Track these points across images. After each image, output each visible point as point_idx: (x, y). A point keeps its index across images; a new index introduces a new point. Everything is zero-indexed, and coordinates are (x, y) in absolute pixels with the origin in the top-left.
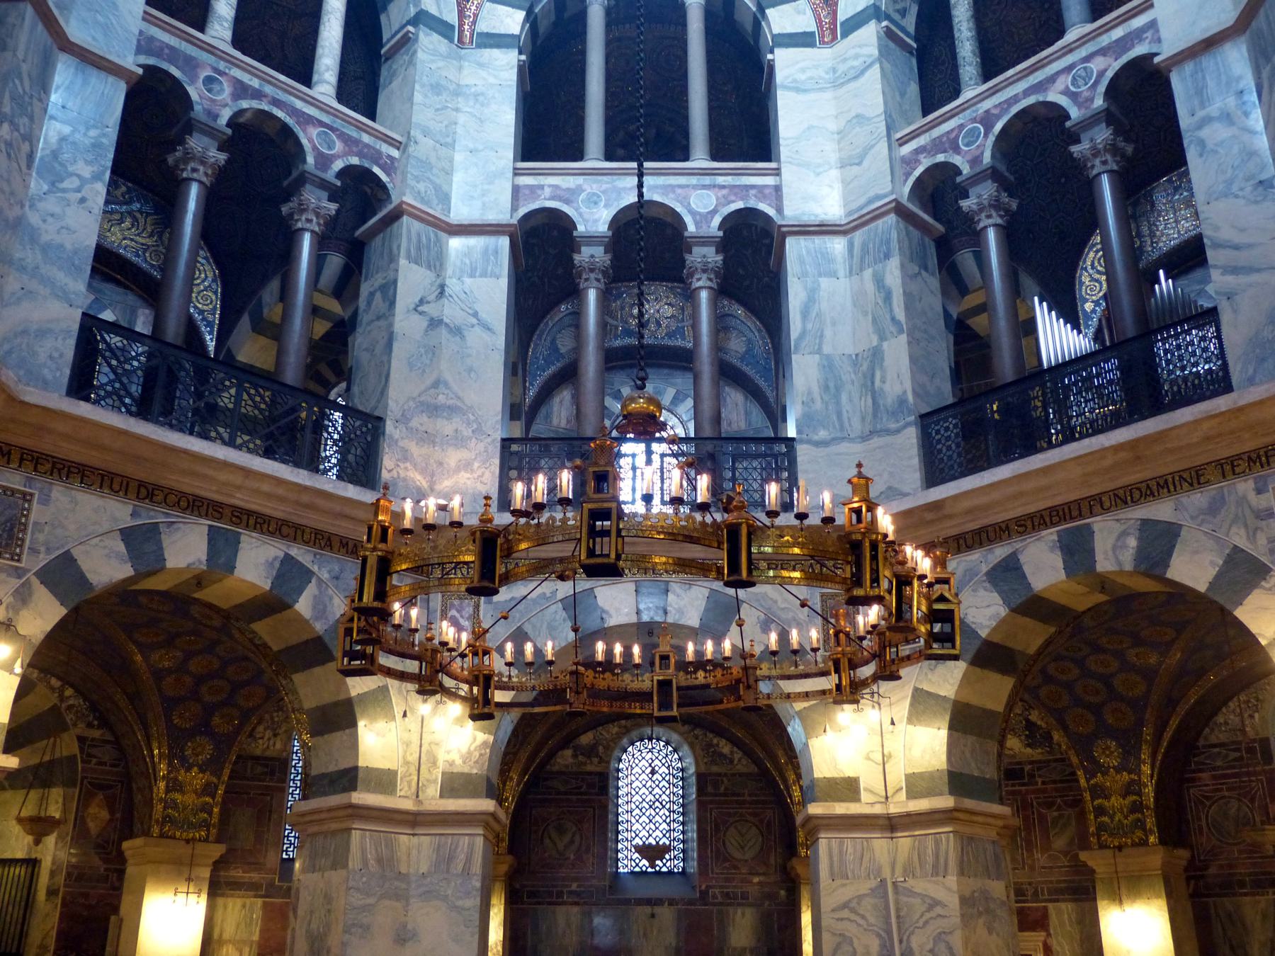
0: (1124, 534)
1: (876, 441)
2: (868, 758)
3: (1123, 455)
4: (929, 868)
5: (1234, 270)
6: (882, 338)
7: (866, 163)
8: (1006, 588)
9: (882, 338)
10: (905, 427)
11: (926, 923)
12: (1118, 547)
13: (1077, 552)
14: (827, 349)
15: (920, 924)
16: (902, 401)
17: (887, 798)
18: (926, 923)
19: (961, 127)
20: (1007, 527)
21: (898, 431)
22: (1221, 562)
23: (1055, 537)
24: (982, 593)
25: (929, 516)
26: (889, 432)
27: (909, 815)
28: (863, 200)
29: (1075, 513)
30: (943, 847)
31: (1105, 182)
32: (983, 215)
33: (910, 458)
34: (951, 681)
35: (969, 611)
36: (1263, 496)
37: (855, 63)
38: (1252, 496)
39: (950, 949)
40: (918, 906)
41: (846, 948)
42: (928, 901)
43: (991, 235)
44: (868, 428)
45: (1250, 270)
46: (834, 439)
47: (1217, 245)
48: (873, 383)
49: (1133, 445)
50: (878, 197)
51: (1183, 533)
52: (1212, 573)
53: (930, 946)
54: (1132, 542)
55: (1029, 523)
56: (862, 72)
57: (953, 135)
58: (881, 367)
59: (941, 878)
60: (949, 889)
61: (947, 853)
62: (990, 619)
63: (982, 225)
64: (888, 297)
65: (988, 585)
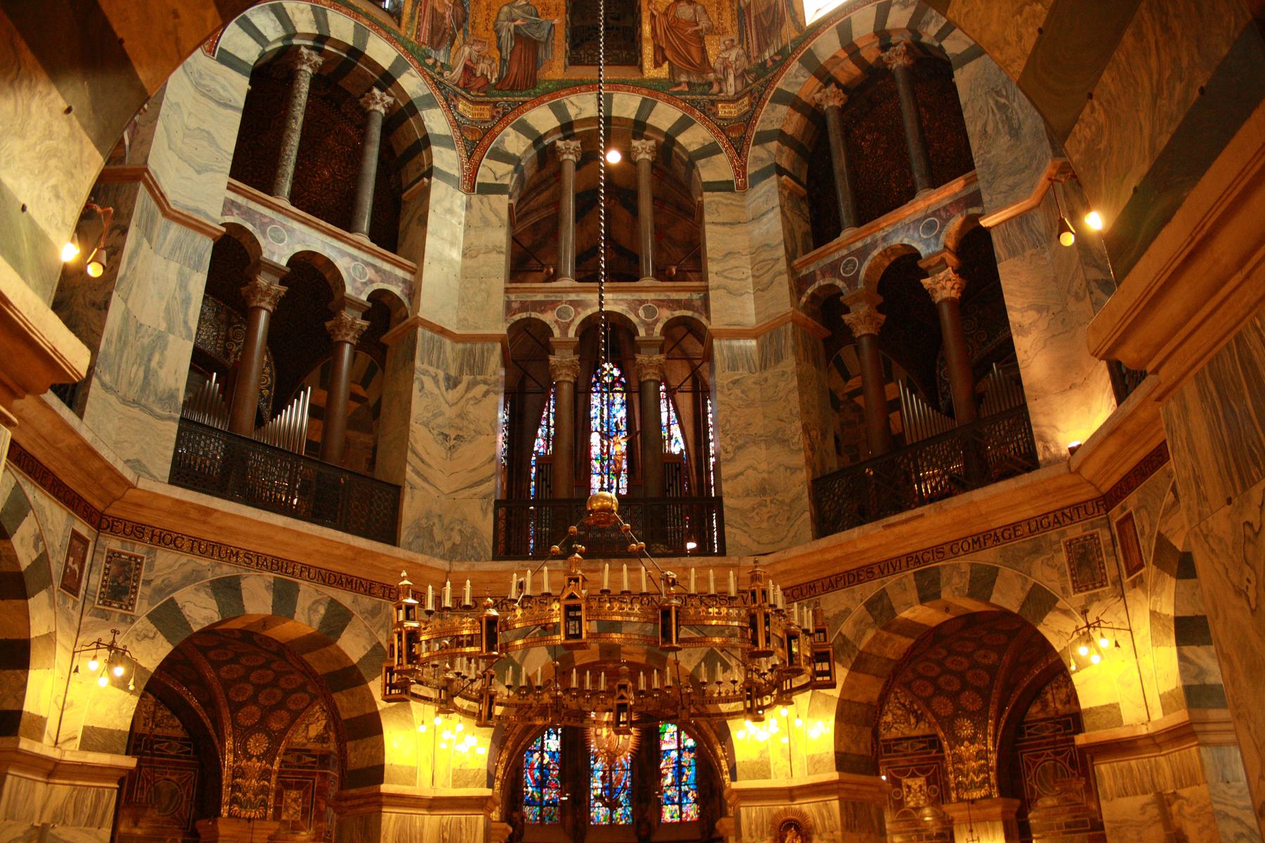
1: (136, 412)
3: (350, 553)
5: (418, 473)
6: (170, 329)
7: (206, 177)
9: (170, 329)
10: (171, 418)
12: (312, 609)
13: (285, 597)
14: (130, 305)
16: (172, 396)
19: (272, 221)
21: (162, 418)
24: (203, 595)
25: (193, 514)
26: (152, 413)
27: (83, 765)
28: (191, 204)
29: (290, 570)
31: (347, 347)
32: (268, 299)
33: (166, 448)
37: (221, 91)
43: (263, 316)
44: (132, 394)
45: (425, 480)
46: (111, 388)
47: (414, 452)
48: (150, 360)
49: (360, 552)
50: (207, 216)
52: (362, 653)
54: (322, 611)
55: (254, 559)
56: (226, 105)
57: (267, 220)
58: (162, 354)
62: (204, 618)
63: (263, 304)
64: (187, 301)
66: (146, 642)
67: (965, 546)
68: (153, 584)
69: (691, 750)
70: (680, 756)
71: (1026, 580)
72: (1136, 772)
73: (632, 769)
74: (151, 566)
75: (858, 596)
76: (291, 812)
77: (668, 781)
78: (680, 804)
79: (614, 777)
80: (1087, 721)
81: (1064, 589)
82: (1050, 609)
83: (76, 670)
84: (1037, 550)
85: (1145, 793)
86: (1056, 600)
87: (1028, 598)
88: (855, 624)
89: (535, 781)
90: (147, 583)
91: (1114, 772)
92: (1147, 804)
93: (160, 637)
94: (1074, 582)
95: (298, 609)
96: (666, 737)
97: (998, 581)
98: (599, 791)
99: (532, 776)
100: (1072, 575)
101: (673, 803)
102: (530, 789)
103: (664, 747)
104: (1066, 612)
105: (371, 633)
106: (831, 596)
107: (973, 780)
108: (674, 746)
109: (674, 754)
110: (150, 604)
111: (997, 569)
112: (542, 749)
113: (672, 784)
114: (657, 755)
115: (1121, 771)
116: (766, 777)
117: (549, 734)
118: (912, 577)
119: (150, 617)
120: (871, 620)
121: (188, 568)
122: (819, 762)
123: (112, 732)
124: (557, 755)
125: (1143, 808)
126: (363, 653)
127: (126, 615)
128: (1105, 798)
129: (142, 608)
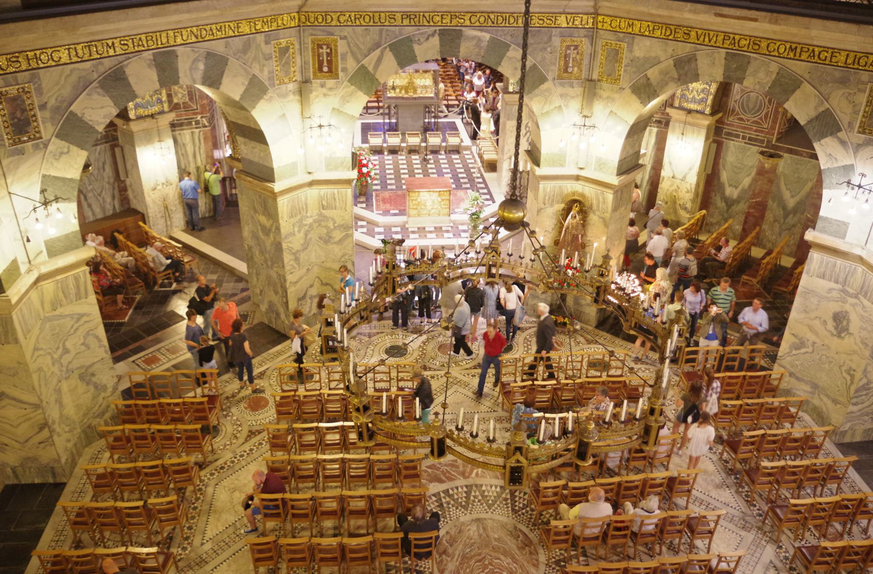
0: (196, 60)
2: (15, 240)
4: (73, 297)
8: (115, 94)
11: (77, 329)
15: (72, 331)
17: (30, 262)
18: (77, 329)
20: (113, 44)
22: (247, 83)
23: (151, 57)
24: (95, 96)
30: (82, 280)
34: (76, 166)
35: (85, 111)
36: (269, 46)
38: (263, 45)
39: (97, 338)
40: (68, 322)
41: (42, 374)
42: (76, 317)
51: (229, 63)
53: (82, 341)
54: (201, 66)
59: (84, 300)
60: (91, 304)
61: (85, 283)
62: (104, 117)
65: (100, 90)
66: (64, 156)
67: (782, 50)
68: (49, 106)
71: (823, 103)
72: (837, 269)
74: (39, 91)
75: (670, 51)
76: (180, 96)
80: (819, 224)
81: (850, 124)
82: (831, 134)
83: (28, 240)
84: (843, 82)
85: (837, 282)
86: (840, 130)
87: (817, 118)
88: (661, 73)
90: (43, 107)
91: (822, 262)
92: (834, 289)
93: (74, 149)
94: (862, 122)
95: (181, 75)
97: (798, 92)
100: (863, 116)
104: (843, 143)
105: (246, 70)
106: (647, 42)
107: (694, 97)
110: (53, 125)
111: (802, 82)
115: (828, 264)
116: (562, 165)
118: (724, 56)
119: (57, 136)
120: (676, 76)
121: (74, 78)
122: (604, 164)
123: (67, 236)
125: (830, 290)
126: (243, 89)
127: (37, 144)
128: (807, 273)
129: (47, 130)
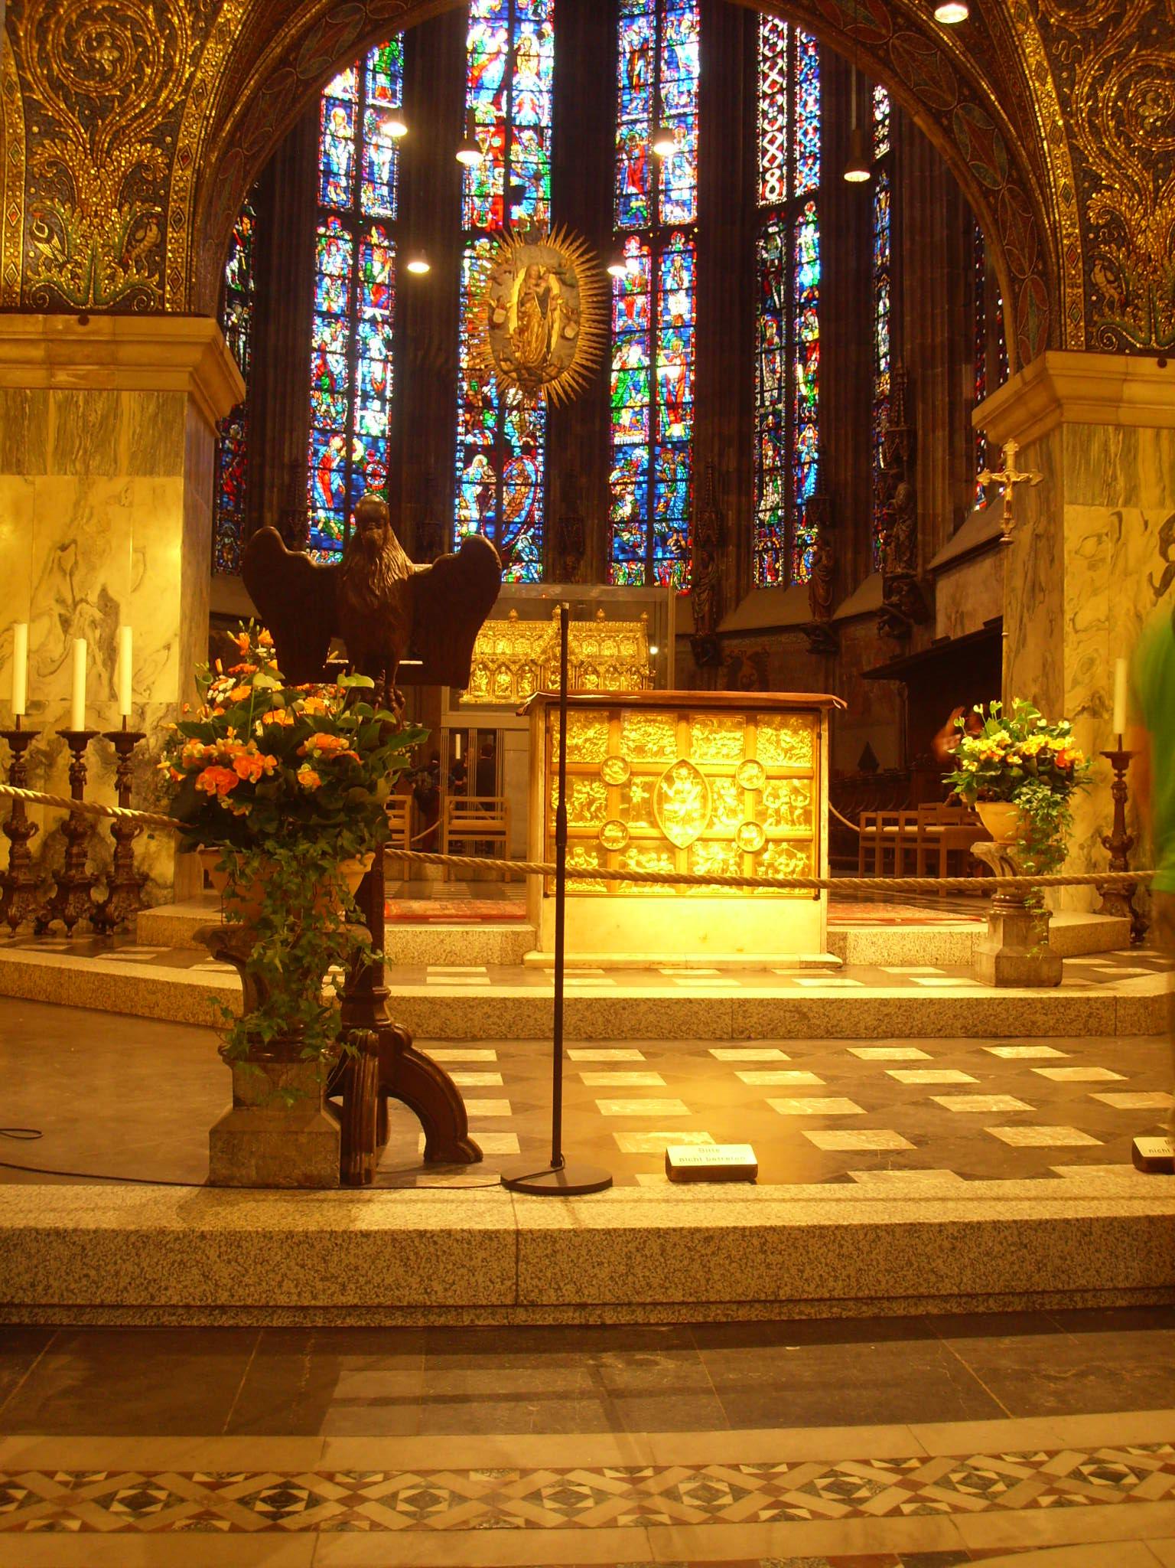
69: (679, 446)
70: (653, 458)
73: (546, 484)
77: (625, 510)
78: (649, 561)
79: (506, 499)
89: (333, 496)
96: (625, 417)
98: (473, 527)
99: (327, 486)
101: (636, 559)
102: (321, 514)
103: (619, 439)
108: (638, 437)
109: (641, 454)
112: (349, 432)
113: (634, 518)
114: (606, 453)
117: (366, 396)
124: (382, 444)
